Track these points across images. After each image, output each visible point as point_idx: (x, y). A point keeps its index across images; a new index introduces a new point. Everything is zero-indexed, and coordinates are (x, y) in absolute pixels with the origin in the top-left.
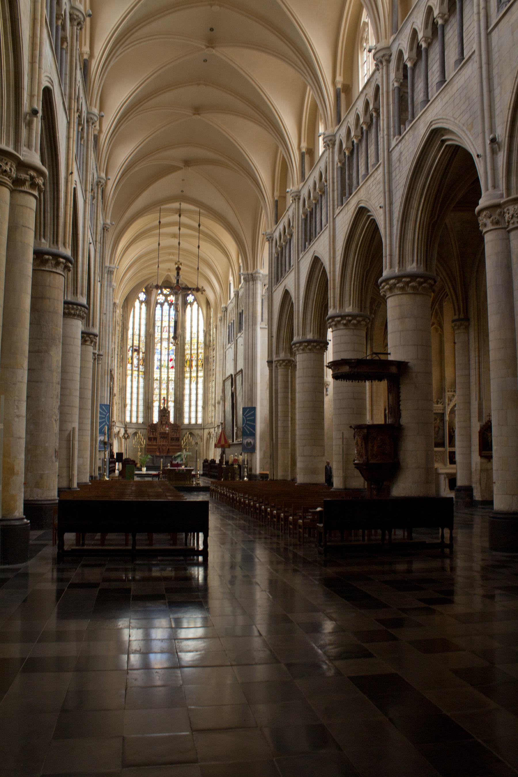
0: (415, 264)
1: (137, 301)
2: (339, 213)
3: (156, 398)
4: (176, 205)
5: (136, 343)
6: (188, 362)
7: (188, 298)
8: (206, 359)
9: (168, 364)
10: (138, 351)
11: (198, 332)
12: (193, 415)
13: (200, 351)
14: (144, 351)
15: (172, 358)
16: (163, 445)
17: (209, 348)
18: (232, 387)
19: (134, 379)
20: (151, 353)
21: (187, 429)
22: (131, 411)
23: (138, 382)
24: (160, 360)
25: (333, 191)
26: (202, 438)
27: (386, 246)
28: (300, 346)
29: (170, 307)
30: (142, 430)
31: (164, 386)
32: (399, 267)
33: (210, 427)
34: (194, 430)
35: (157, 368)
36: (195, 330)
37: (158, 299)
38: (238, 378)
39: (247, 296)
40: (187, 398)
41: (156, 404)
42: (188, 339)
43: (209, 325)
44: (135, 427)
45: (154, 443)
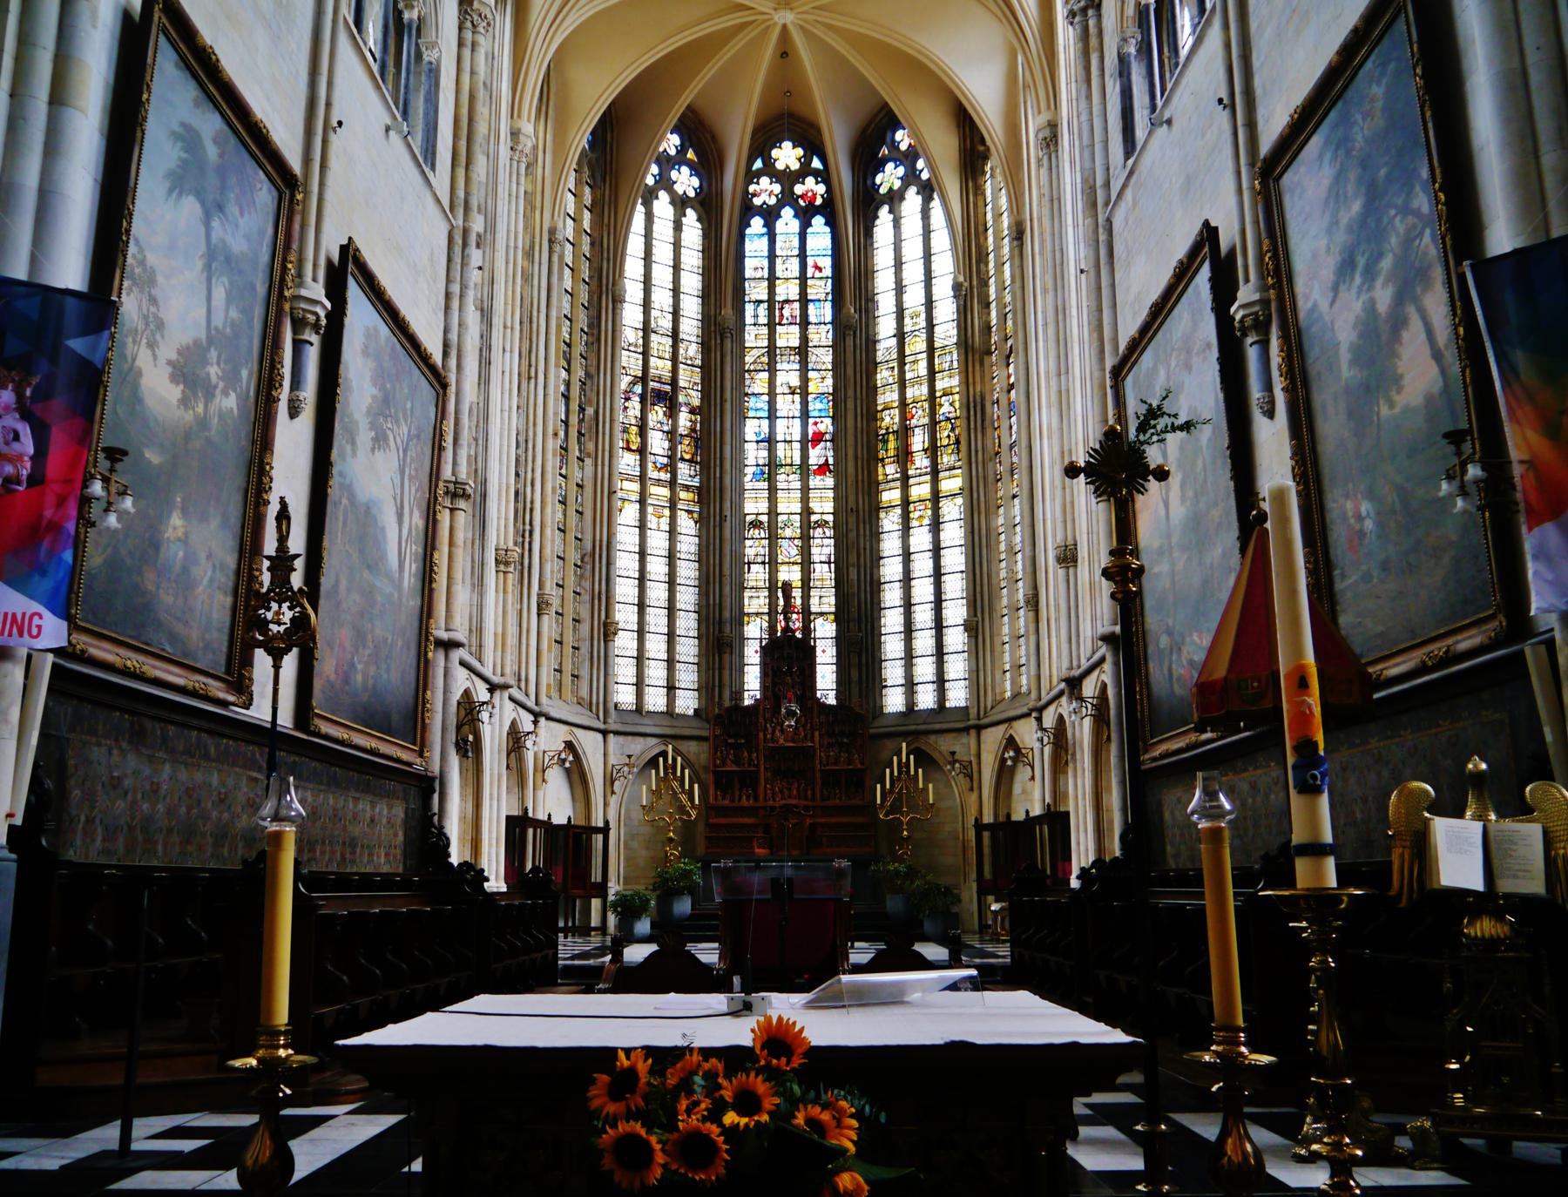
3: (756, 602)
5: (660, 366)
6: (891, 437)
7: (878, 180)
8: (976, 409)
9: (805, 456)
10: (669, 400)
11: (929, 304)
12: (925, 669)
14: (696, 402)
15: (822, 428)
16: (787, 809)
17: (986, 359)
19: (652, 521)
20: (728, 406)
22: (640, 659)
23: (673, 532)
24: (771, 441)
29: (805, 225)
30: (692, 748)
31: (788, 550)
33: (1012, 713)
34: (933, 738)
36: (914, 298)
37: (754, 195)
40: (892, 596)
41: (754, 630)
42: (886, 345)
43: (979, 262)
45: (744, 802)
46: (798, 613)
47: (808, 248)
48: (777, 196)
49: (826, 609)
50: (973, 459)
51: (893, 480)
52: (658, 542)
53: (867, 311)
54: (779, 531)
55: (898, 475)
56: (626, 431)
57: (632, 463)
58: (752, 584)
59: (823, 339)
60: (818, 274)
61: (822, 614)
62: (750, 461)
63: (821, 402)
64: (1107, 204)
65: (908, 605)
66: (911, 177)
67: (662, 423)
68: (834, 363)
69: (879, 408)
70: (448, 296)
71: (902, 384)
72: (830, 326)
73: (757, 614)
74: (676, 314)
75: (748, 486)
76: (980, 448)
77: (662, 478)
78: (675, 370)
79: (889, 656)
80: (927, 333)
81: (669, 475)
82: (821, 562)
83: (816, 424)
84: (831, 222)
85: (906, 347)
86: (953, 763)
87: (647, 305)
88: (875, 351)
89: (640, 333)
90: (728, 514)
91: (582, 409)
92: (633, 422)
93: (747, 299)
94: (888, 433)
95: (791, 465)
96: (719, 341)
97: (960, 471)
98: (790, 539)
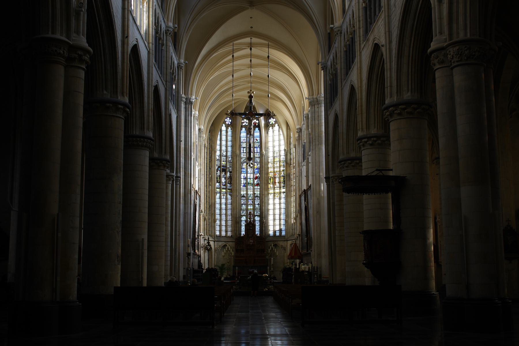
0: (409, 93)
1: (224, 125)
2: (363, 48)
4: (247, 40)
6: (272, 179)
7: (270, 120)
9: (254, 182)
11: (280, 151)
15: (257, 175)
18: (305, 202)
20: (238, 172)
21: (272, 241)
22: (220, 226)
25: (359, 28)
26: (285, 249)
27: (387, 78)
28: (344, 164)
29: (254, 130)
30: (231, 243)
31: (250, 202)
32: (397, 96)
34: (278, 242)
35: (244, 186)
36: (277, 149)
37: (243, 123)
38: (309, 192)
39: (313, 118)
40: (271, 212)
41: (244, 218)
43: (290, 145)
44: (224, 240)
46: (252, 215)
49: (258, 214)
52: (223, 201)
53: (267, 151)
59: (258, 156)
60: (257, 141)
61: (257, 215)
62: (242, 183)
64: (301, 166)
65: (274, 215)
66: (276, 122)
67: (224, 176)
68: (260, 161)
69: (269, 172)
70: (199, 180)
71: (274, 168)
72: (259, 153)
73: (244, 215)
74: (227, 151)
75: (242, 188)
76: (289, 184)
78: (226, 164)
83: (256, 175)
84: (260, 130)
86: (282, 247)
87: (221, 150)
89: (219, 157)
90: (237, 195)
91: (209, 176)
92: (218, 176)
95: (251, 184)
98: (250, 200)
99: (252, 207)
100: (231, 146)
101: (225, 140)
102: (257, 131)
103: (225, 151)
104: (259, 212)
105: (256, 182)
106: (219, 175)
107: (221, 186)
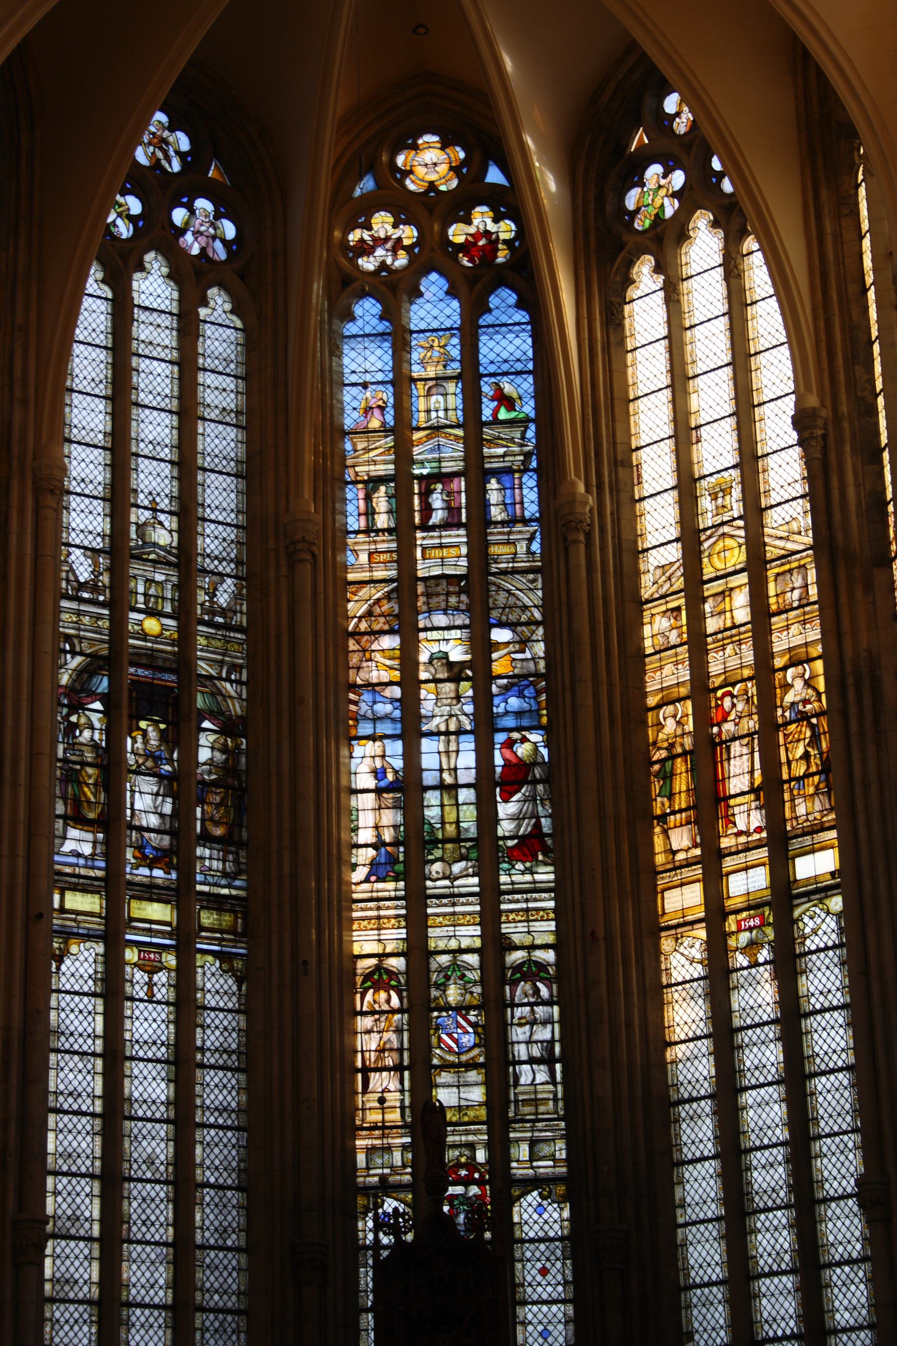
6: (680, 766)
7: (632, 199)
13: (780, 643)
14: (236, 708)
15: (523, 750)
37: (364, 249)
47: (483, 360)
48: (408, 249)
49: (545, 1167)
50: (860, 805)
51: (688, 864)
53: (615, 488)
54: (434, 993)
55: (698, 852)
56: (72, 777)
57: (87, 849)
58: (374, 1117)
60: (503, 414)
62: (365, 836)
63: (521, 695)
67: (157, 759)
68: (546, 606)
69: (652, 701)
72: (534, 527)
75: (361, 891)
77: (160, 881)
78: (185, 638)
79: (696, 1275)
80: (745, 528)
81: (174, 876)
82: (532, 1061)
83: (509, 744)
85: (705, 560)
88: (637, 574)
92: (89, 756)
93: (349, 475)
94: (672, 757)
95: (457, 840)
96: (284, 571)
97: (833, 834)
99: (477, 1094)
100: (231, 467)
101: (174, 405)
102: (504, 319)
103: (164, 504)
104: (561, 1144)
105: (517, 818)
106: (95, 746)
107: (124, 861)
